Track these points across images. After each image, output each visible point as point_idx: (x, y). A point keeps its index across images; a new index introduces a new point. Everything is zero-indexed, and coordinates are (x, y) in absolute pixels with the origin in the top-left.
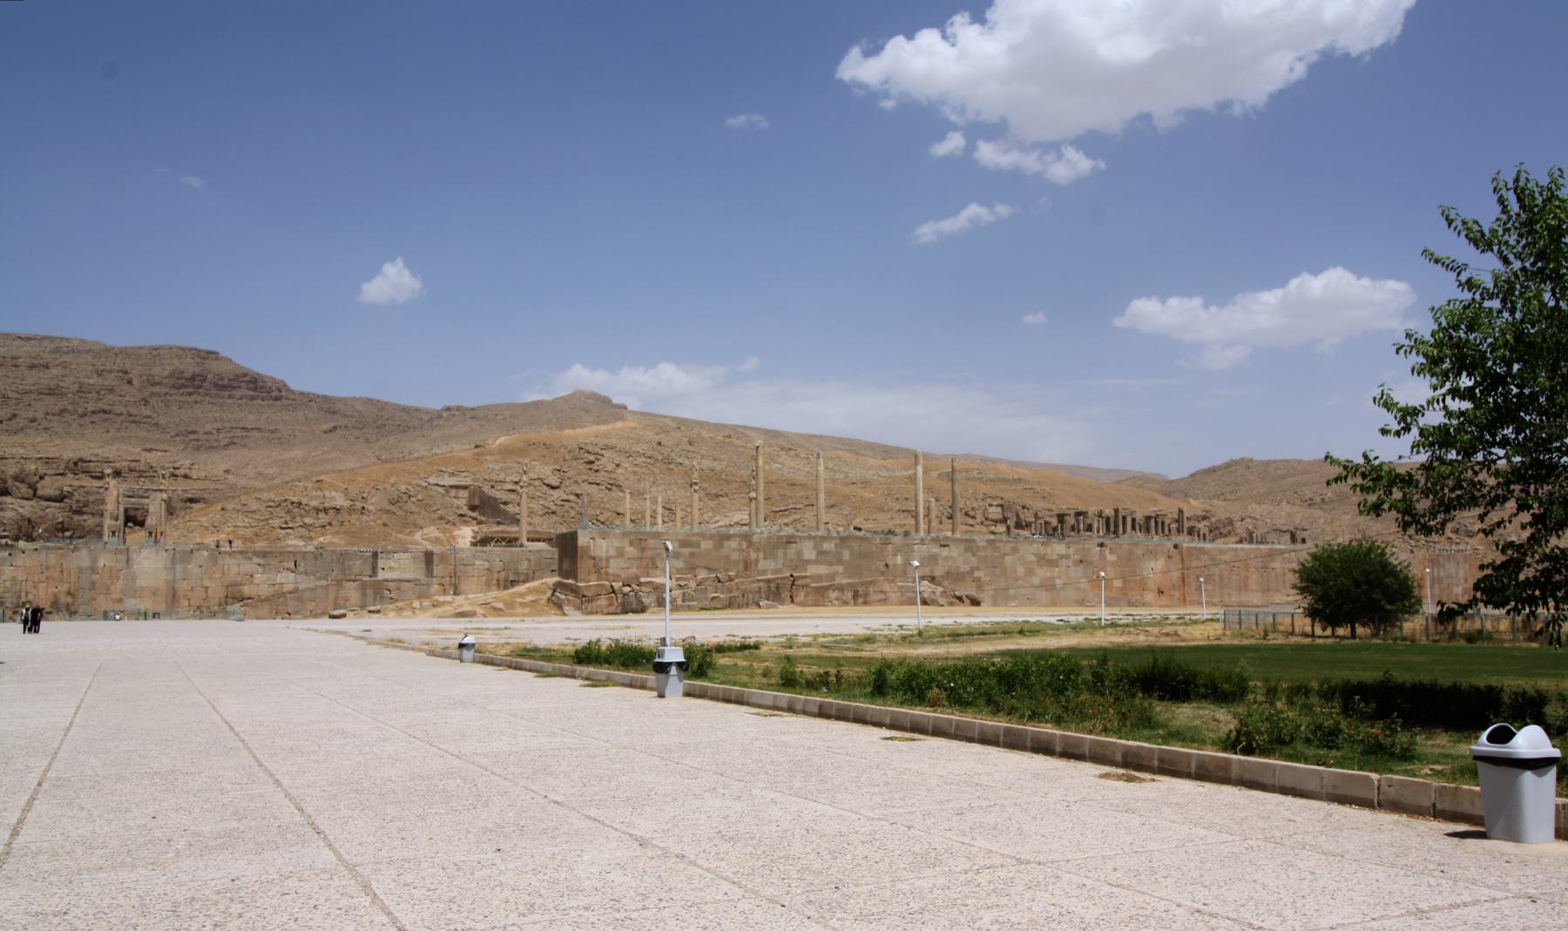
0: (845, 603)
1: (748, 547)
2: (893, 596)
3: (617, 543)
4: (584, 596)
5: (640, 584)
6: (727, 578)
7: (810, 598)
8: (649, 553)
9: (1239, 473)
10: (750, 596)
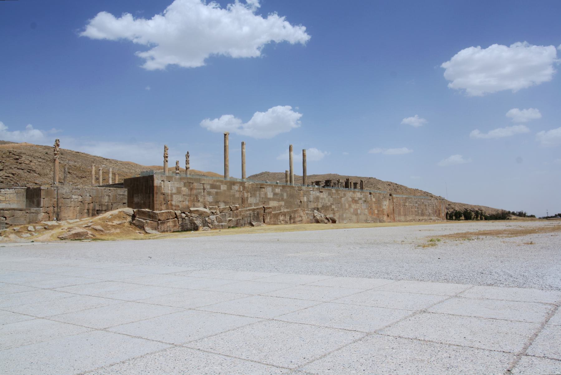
0: (286, 223)
1: (243, 190)
2: (305, 218)
3: (177, 185)
4: (159, 220)
5: (191, 212)
6: (235, 208)
7: (272, 220)
8: (194, 192)
9: (266, 177)
10: (246, 219)
